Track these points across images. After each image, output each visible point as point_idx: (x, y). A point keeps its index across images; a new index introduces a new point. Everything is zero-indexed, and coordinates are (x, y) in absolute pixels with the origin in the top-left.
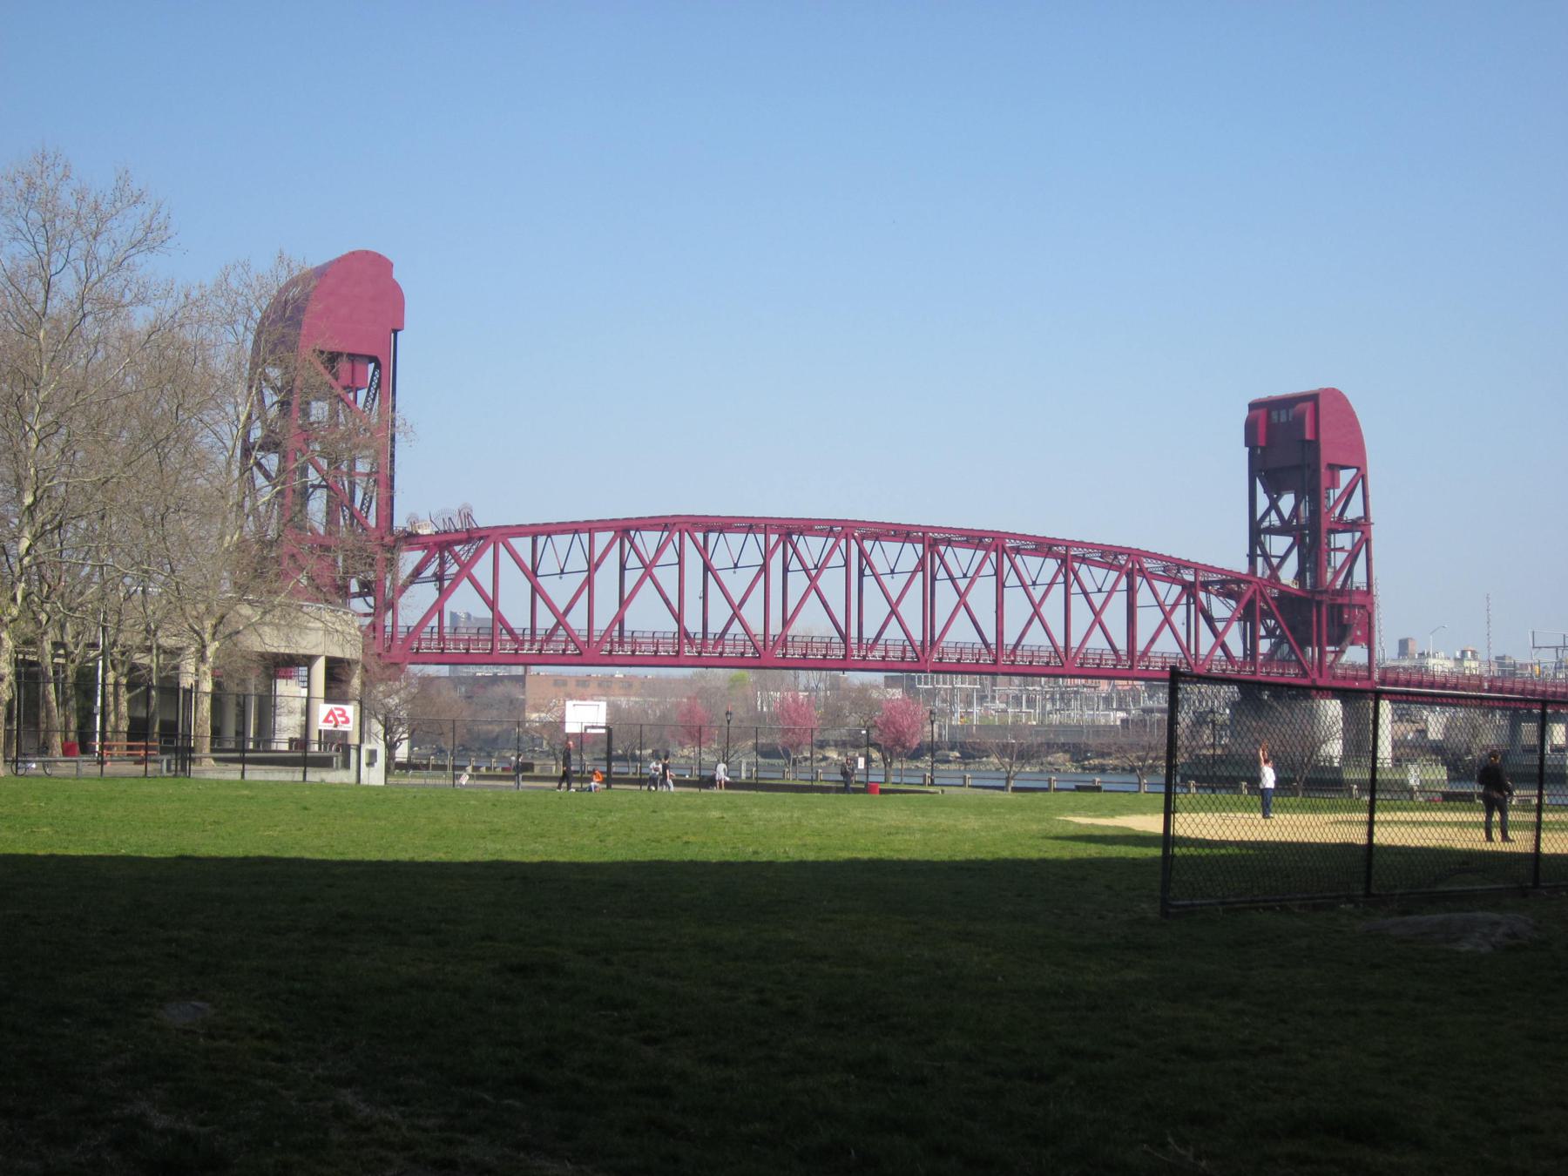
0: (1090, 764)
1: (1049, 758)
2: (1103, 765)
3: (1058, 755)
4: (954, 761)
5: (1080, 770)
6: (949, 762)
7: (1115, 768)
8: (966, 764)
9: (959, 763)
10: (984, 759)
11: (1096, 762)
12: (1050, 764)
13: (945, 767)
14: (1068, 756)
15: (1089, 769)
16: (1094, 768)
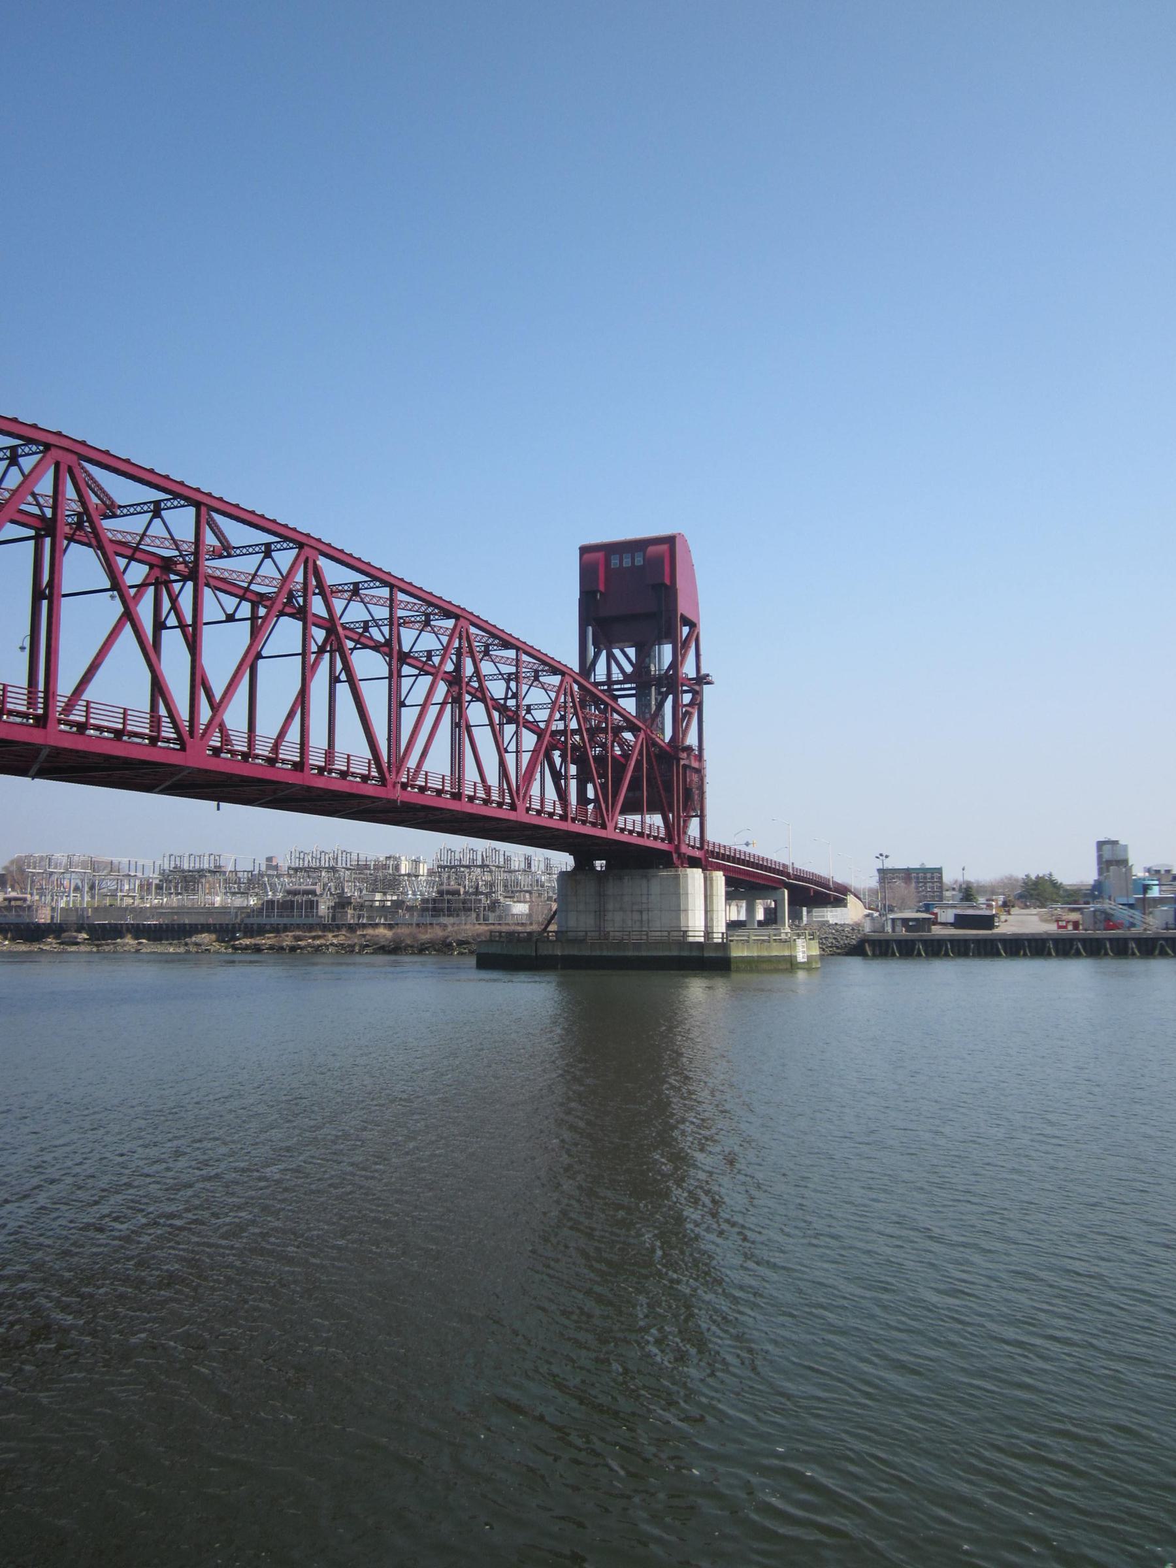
0: (241, 944)
1: (194, 939)
2: (255, 945)
3: (203, 935)
4: (83, 943)
5: (230, 950)
6: (77, 944)
7: (271, 948)
8: (98, 946)
9: (89, 944)
10: (119, 940)
11: (247, 941)
12: (197, 944)
13: (74, 948)
14: (213, 937)
15: (241, 949)
16: (247, 948)
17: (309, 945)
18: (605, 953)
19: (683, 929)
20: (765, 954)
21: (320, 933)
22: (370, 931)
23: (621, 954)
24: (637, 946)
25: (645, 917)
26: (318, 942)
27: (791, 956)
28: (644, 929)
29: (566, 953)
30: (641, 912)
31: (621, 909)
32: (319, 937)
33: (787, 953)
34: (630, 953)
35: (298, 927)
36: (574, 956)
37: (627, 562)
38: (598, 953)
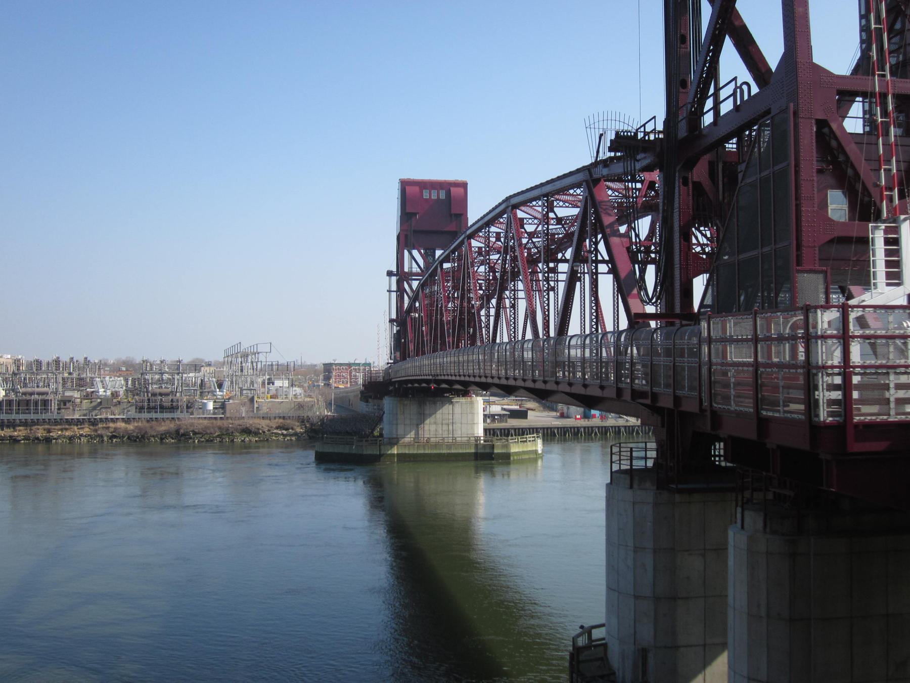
17: (59, 437)
18: (427, 452)
19: (476, 435)
20: (525, 449)
21: (67, 427)
22: (111, 425)
23: (438, 451)
24: (449, 446)
25: (451, 427)
26: (67, 433)
27: (536, 450)
28: (450, 436)
29: (400, 452)
30: (448, 425)
31: (435, 423)
32: (66, 429)
33: (534, 449)
34: (445, 451)
35: (49, 422)
36: (405, 454)
37: (434, 196)
38: (421, 451)
